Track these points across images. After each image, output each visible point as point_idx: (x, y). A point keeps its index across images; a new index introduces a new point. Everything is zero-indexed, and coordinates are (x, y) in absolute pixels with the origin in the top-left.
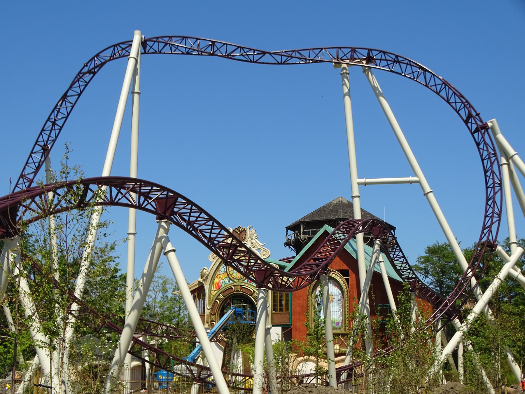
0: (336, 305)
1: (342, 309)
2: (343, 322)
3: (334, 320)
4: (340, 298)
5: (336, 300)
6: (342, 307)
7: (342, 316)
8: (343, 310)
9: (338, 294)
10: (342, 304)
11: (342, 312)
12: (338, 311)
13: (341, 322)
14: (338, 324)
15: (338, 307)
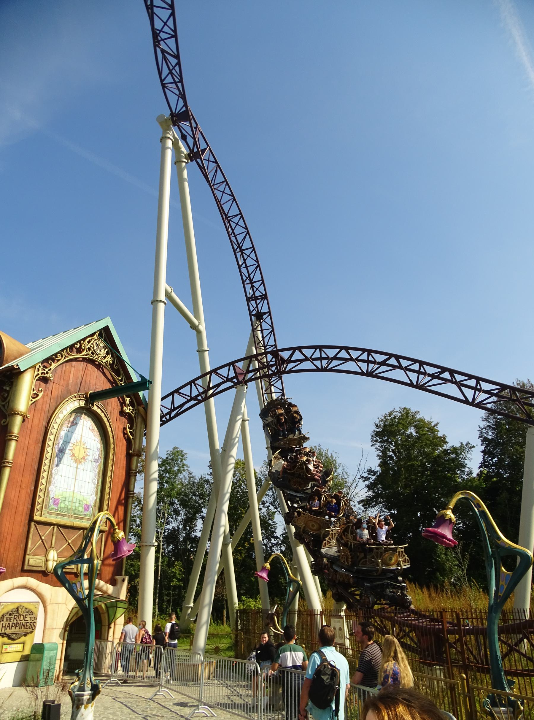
0: (89, 469)
1: (98, 480)
2: (95, 506)
3: (81, 499)
4: (97, 457)
5: (90, 458)
6: (99, 476)
7: (96, 494)
8: (98, 482)
9: (95, 449)
10: (99, 471)
11: (97, 486)
12: (91, 481)
13: (92, 504)
14: (87, 508)
15: (92, 475)
